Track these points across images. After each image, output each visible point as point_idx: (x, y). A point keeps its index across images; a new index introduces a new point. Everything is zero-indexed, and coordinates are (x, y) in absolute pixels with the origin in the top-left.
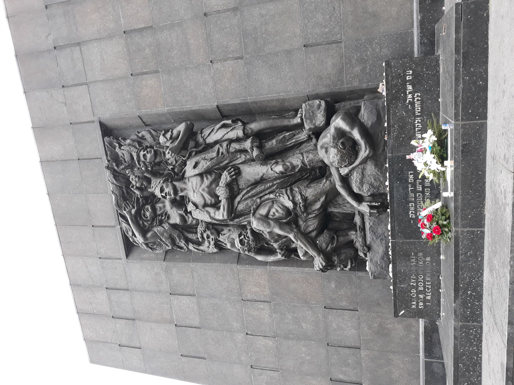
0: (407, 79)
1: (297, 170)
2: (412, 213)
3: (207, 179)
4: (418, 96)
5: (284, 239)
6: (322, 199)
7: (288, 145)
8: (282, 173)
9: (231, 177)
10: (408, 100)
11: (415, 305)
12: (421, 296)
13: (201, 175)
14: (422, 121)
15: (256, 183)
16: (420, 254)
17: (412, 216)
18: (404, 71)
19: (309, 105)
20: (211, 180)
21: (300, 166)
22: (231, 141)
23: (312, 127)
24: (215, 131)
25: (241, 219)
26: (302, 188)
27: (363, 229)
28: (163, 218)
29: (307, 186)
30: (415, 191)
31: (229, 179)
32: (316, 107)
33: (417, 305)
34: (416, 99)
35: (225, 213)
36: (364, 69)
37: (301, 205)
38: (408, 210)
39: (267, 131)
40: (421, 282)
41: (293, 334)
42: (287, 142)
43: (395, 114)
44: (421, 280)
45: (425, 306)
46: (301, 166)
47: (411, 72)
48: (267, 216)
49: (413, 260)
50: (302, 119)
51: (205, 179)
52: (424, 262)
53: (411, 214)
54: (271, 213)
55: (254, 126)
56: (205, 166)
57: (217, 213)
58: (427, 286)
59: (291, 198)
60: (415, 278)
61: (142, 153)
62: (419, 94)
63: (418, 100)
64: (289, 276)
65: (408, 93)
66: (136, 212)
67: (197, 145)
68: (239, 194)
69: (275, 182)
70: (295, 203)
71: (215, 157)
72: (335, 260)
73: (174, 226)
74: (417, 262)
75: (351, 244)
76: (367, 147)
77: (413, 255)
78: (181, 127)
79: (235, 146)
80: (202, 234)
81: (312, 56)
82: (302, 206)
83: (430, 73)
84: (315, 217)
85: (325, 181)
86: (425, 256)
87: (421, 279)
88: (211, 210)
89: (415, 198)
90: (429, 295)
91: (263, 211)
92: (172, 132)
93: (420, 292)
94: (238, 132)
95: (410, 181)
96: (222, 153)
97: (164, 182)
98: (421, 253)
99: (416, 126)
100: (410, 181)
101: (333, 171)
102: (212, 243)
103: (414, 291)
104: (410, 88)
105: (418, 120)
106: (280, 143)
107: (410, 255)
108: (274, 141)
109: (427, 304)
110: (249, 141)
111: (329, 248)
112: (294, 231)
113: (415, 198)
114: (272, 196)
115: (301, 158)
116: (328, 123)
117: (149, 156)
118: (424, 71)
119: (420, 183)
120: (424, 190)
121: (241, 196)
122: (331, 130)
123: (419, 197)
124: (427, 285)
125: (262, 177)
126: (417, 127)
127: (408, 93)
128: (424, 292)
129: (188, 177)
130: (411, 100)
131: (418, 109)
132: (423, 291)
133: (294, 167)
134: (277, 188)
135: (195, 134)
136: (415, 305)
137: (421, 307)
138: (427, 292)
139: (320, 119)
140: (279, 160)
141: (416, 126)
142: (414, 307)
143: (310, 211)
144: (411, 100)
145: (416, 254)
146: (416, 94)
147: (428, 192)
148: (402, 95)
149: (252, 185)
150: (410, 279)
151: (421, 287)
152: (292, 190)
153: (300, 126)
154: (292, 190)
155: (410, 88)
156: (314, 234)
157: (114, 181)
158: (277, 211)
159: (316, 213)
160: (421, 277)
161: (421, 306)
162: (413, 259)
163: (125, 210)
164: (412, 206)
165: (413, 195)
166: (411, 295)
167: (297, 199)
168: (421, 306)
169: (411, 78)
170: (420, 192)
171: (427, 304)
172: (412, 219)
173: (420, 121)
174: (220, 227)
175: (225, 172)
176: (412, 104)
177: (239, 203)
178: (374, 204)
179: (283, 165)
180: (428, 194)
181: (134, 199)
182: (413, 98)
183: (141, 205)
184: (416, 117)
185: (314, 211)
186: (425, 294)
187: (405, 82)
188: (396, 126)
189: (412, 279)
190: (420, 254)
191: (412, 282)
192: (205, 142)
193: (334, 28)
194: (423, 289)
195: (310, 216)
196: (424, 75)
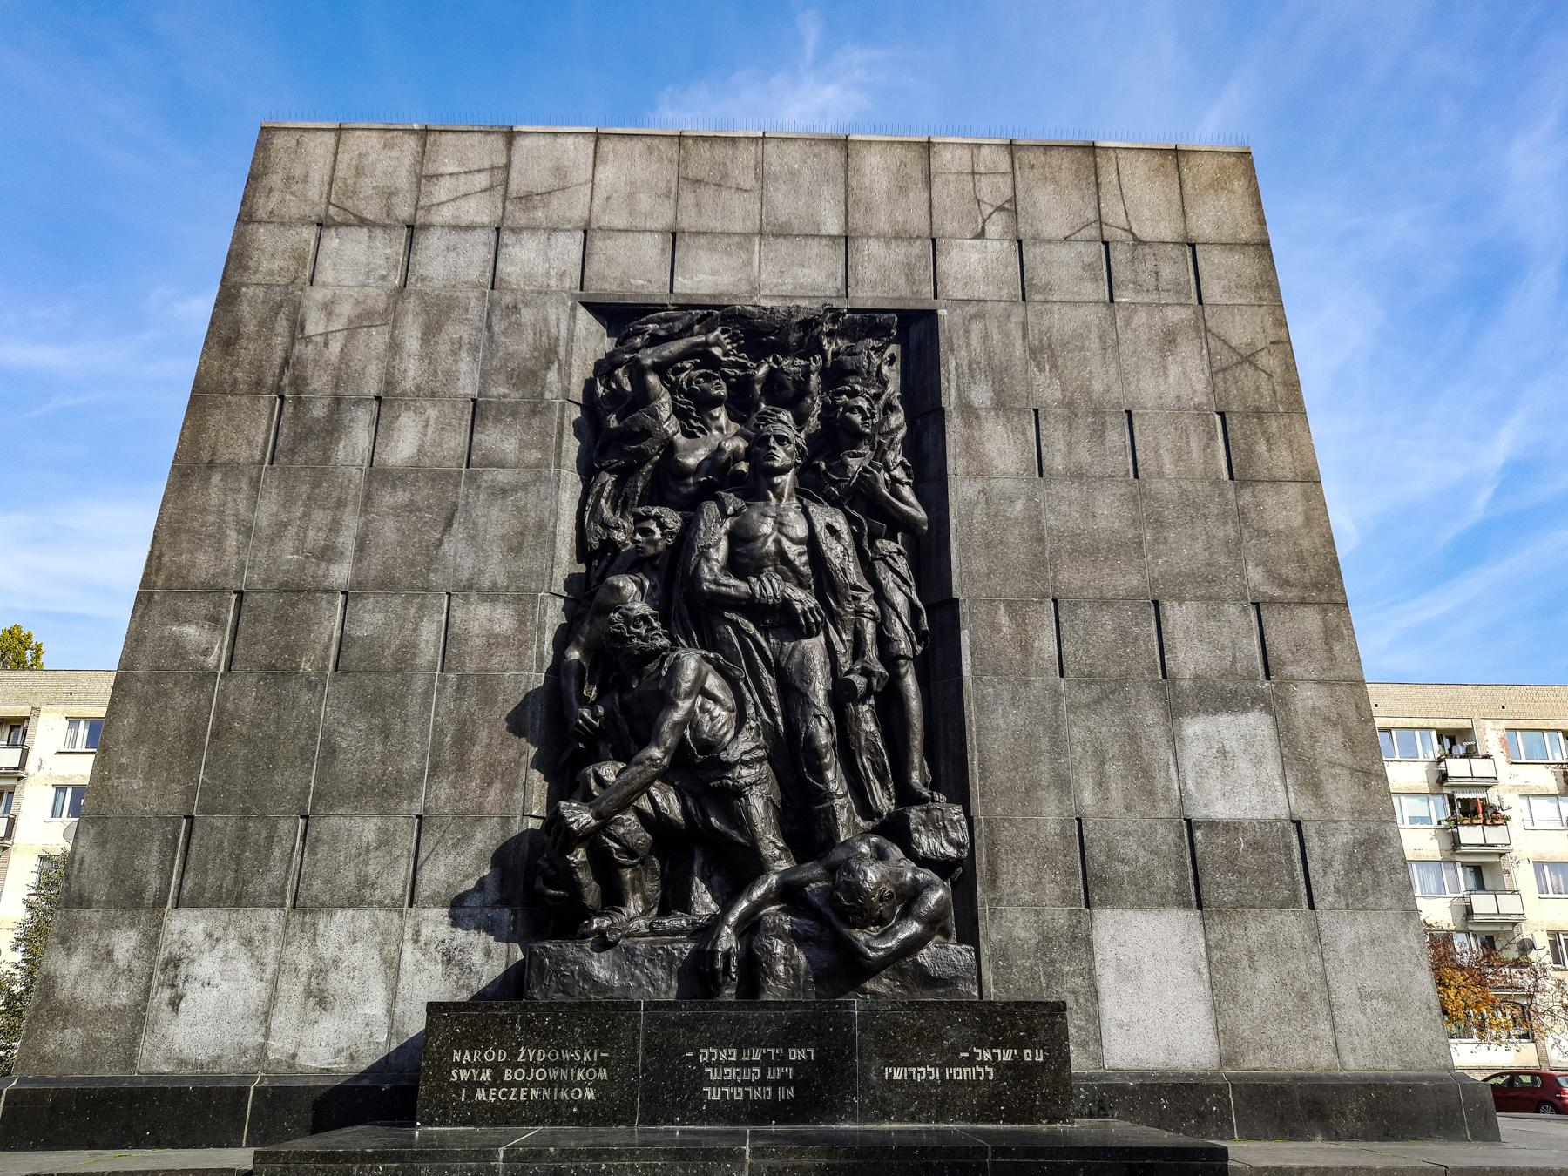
0: (1026, 1051)
2: (712, 1055)
3: (800, 554)
4: (987, 1074)
5: (627, 727)
6: (734, 834)
7: (861, 759)
8: (811, 738)
9: (804, 612)
10: (979, 1051)
11: (461, 1058)
12: (486, 1075)
13: (812, 542)
14: (933, 1084)
16: (603, 1074)
17: (704, 1055)
18: (1042, 1045)
19: (958, 820)
20: (797, 563)
21: (822, 786)
22: (882, 625)
23: (912, 826)
24: (904, 588)
25: (688, 622)
26: (766, 788)
28: (692, 422)
30: (766, 1062)
31: (799, 607)
32: (954, 835)
33: (459, 1065)
34: (982, 1070)
35: (713, 587)
37: (730, 783)
38: (721, 1046)
40: (528, 1074)
42: (867, 758)
43: (951, 1020)
44: (532, 1074)
45: (458, 1086)
46: (822, 791)
47: (1041, 1059)
49: (586, 1056)
51: (803, 548)
52: (582, 1084)
53: (710, 1053)
54: (710, 705)
55: (910, 682)
58: (514, 1090)
59: (747, 758)
60: (540, 1060)
62: (991, 1078)
63: (978, 1074)
65: (994, 1051)
67: (873, 537)
68: (757, 627)
69: (779, 719)
70: (733, 765)
72: (575, 856)
74: (581, 1066)
76: (881, 953)
77: (602, 1055)
80: (657, 518)
82: (727, 784)
83: (1038, 1103)
85: (781, 845)
86: (597, 1085)
87: (535, 1074)
88: (720, 554)
89: (751, 1064)
90: (487, 1096)
91: (713, 682)
93: (497, 1069)
94: (904, 647)
95: (790, 1051)
97: (798, 446)
98: (605, 1073)
99: (920, 1069)
100: (790, 1051)
101: (813, 870)
103: (502, 1055)
104: (1007, 1056)
105: (935, 1073)
106: (867, 740)
107: (601, 1047)
109: (464, 1091)
110: (879, 668)
111: (611, 844)
112: (664, 757)
113: (751, 1064)
116: (924, 862)
117: (857, 418)
118: (1041, 1090)
119: (784, 1076)
120: (766, 1086)
121: (752, 629)
122: (924, 875)
123: (752, 1072)
124: (518, 1093)
125: (798, 690)
126: (917, 1072)
127: (994, 1051)
128: (497, 1081)
130: (979, 1059)
131: (958, 1073)
132: (502, 1080)
133: (819, 772)
134: (763, 721)
136: (461, 1058)
137: (455, 1075)
138: (497, 1092)
139: (927, 843)
140: (835, 735)
141: (920, 1069)
142: (457, 1056)
144: (979, 1059)
145: (602, 1063)
146: (991, 1070)
147: (762, 1095)
148: (991, 1039)
149: (777, 661)
150: (537, 1047)
151: (513, 1074)
152: (760, 760)
153: (906, 796)
154: (760, 760)
155: (1007, 1056)
156: (644, 804)
159: (696, 815)
160: (541, 1074)
161: (458, 1074)
162: (591, 1055)
163: (723, 332)
164: (728, 1055)
165: (757, 1057)
166: (490, 1050)
168: (458, 1074)
169: (1028, 1059)
170: (764, 1074)
171: (464, 1091)
172: (697, 1056)
173: (931, 1078)
176: (971, 1061)
177: (735, 625)
178: (734, 961)
179: (826, 745)
180: (757, 1094)
181: (742, 358)
182: (982, 1064)
183: (726, 370)
184: (942, 1067)
186: (492, 1085)
187: (1020, 1045)
188: (922, 1021)
189: (536, 1053)
190: (603, 1074)
191: (526, 1052)
192: (877, 559)
194: (506, 1079)
196: (1032, 1088)
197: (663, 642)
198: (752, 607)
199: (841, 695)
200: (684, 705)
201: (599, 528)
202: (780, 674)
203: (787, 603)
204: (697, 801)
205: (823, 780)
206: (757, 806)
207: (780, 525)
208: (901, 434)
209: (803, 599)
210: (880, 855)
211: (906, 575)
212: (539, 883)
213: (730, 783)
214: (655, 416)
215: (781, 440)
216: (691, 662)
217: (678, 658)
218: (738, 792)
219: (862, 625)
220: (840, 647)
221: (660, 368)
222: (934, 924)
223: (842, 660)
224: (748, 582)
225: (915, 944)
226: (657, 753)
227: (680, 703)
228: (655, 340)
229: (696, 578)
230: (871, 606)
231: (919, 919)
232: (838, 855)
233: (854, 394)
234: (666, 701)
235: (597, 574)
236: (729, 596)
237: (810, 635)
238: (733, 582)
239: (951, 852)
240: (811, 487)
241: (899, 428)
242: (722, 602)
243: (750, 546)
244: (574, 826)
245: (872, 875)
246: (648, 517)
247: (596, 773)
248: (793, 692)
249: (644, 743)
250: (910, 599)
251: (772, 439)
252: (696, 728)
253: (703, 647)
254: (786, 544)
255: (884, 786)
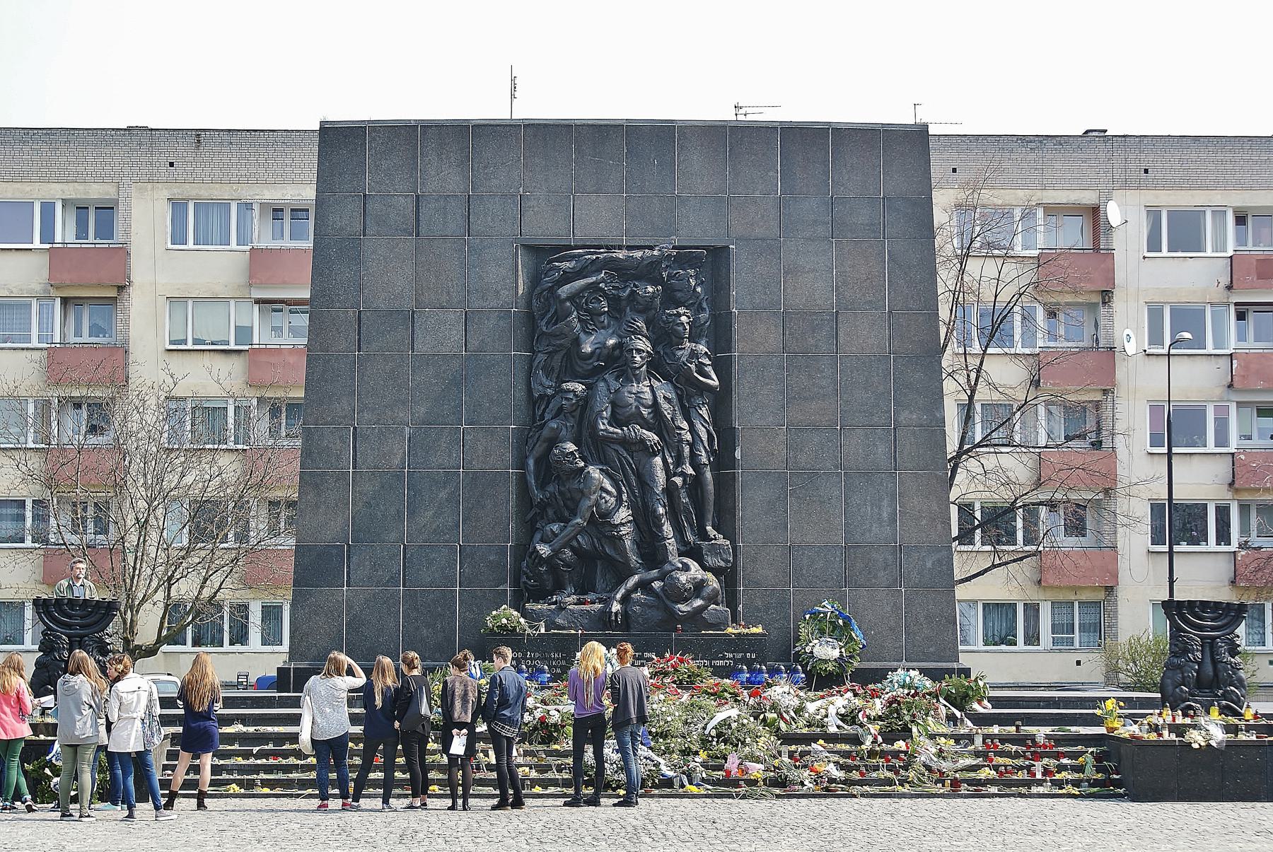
1: (654, 530)
8: (655, 511)
13: (655, 405)
15: (639, 476)
27: (579, 603)
29: (634, 540)
32: (725, 556)
36: (759, 610)
37: (616, 534)
39: (699, 491)
40: (532, 663)
41: (415, 495)
46: (660, 536)
48: (603, 490)
49: (556, 655)
50: (712, 539)
51: (650, 410)
54: (604, 495)
55: (708, 475)
56: (666, 413)
57: (606, 422)
61: (684, 319)
64: (502, 500)
66: (602, 290)
69: (639, 499)
71: (674, 424)
73: (577, 342)
75: (559, 587)
78: (714, 382)
79: (687, 450)
81: (778, 553)
84: (595, 547)
85: (640, 562)
91: (607, 484)
92: (709, 365)
94: (704, 460)
96: (680, 434)
97: (648, 352)
101: (655, 573)
102: (549, 392)
108: (687, 500)
114: (625, 497)
115: (669, 537)
117: (681, 328)
129: (651, 387)
133: (660, 527)
135: (702, 396)
139: (711, 560)
143: (603, 541)
150: (534, 652)
154: (629, 522)
156: (575, 543)
157: (645, 262)
158: (606, 502)
167: (622, 529)
174: (577, 413)
175: (656, 438)
176: (724, 658)
177: (616, 451)
182: (728, 659)
185: (603, 547)
193: (806, 580)
195: (595, 540)
197: (582, 464)
198: (624, 442)
199: (670, 490)
200: (594, 497)
201: (540, 388)
202: (639, 476)
203: (642, 441)
204: (599, 540)
205: (662, 531)
206: (628, 543)
207: (638, 399)
208: (708, 323)
209: (652, 437)
210: (686, 568)
211: (707, 419)
212: (524, 579)
213: (616, 534)
214: (569, 324)
215: (639, 351)
216: (595, 472)
217: (589, 472)
218: (620, 538)
219: (683, 448)
220: (670, 460)
221: (572, 298)
222: (713, 599)
223: (671, 467)
224: (622, 430)
225: (703, 608)
226: (579, 520)
227: (592, 497)
228: (568, 277)
229: (594, 427)
230: (689, 437)
231: (703, 599)
232: (667, 567)
233: (679, 315)
234: (583, 494)
235: (540, 413)
236: (613, 438)
237: (656, 456)
238: (616, 430)
239: (722, 564)
240: (657, 367)
241: (706, 322)
242: (609, 440)
243: (624, 410)
244: (544, 556)
245: (683, 578)
246: (569, 391)
247: (551, 529)
248: (644, 482)
249: (574, 514)
250: (708, 431)
251: (634, 351)
252: (597, 504)
253: (602, 463)
254: (642, 409)
255: (692, 529)
